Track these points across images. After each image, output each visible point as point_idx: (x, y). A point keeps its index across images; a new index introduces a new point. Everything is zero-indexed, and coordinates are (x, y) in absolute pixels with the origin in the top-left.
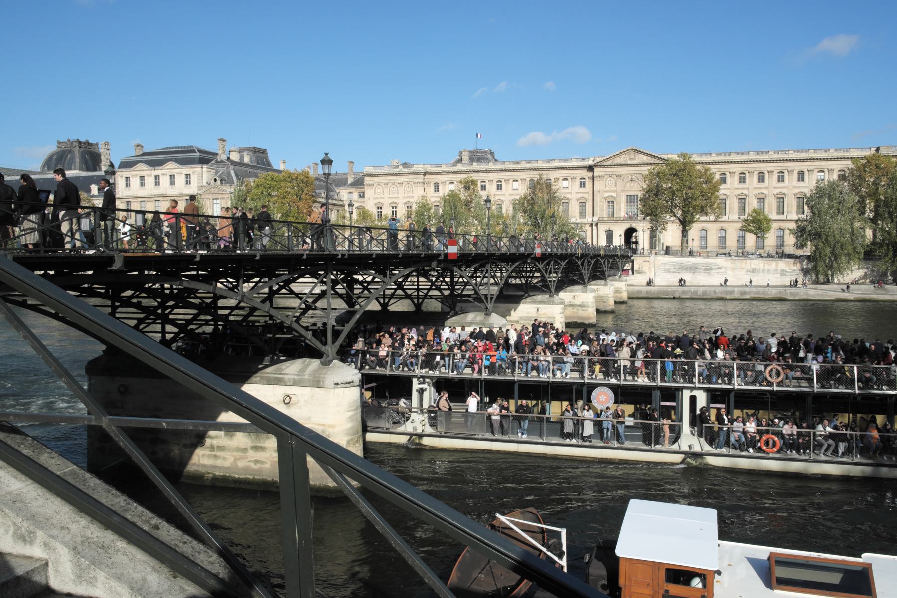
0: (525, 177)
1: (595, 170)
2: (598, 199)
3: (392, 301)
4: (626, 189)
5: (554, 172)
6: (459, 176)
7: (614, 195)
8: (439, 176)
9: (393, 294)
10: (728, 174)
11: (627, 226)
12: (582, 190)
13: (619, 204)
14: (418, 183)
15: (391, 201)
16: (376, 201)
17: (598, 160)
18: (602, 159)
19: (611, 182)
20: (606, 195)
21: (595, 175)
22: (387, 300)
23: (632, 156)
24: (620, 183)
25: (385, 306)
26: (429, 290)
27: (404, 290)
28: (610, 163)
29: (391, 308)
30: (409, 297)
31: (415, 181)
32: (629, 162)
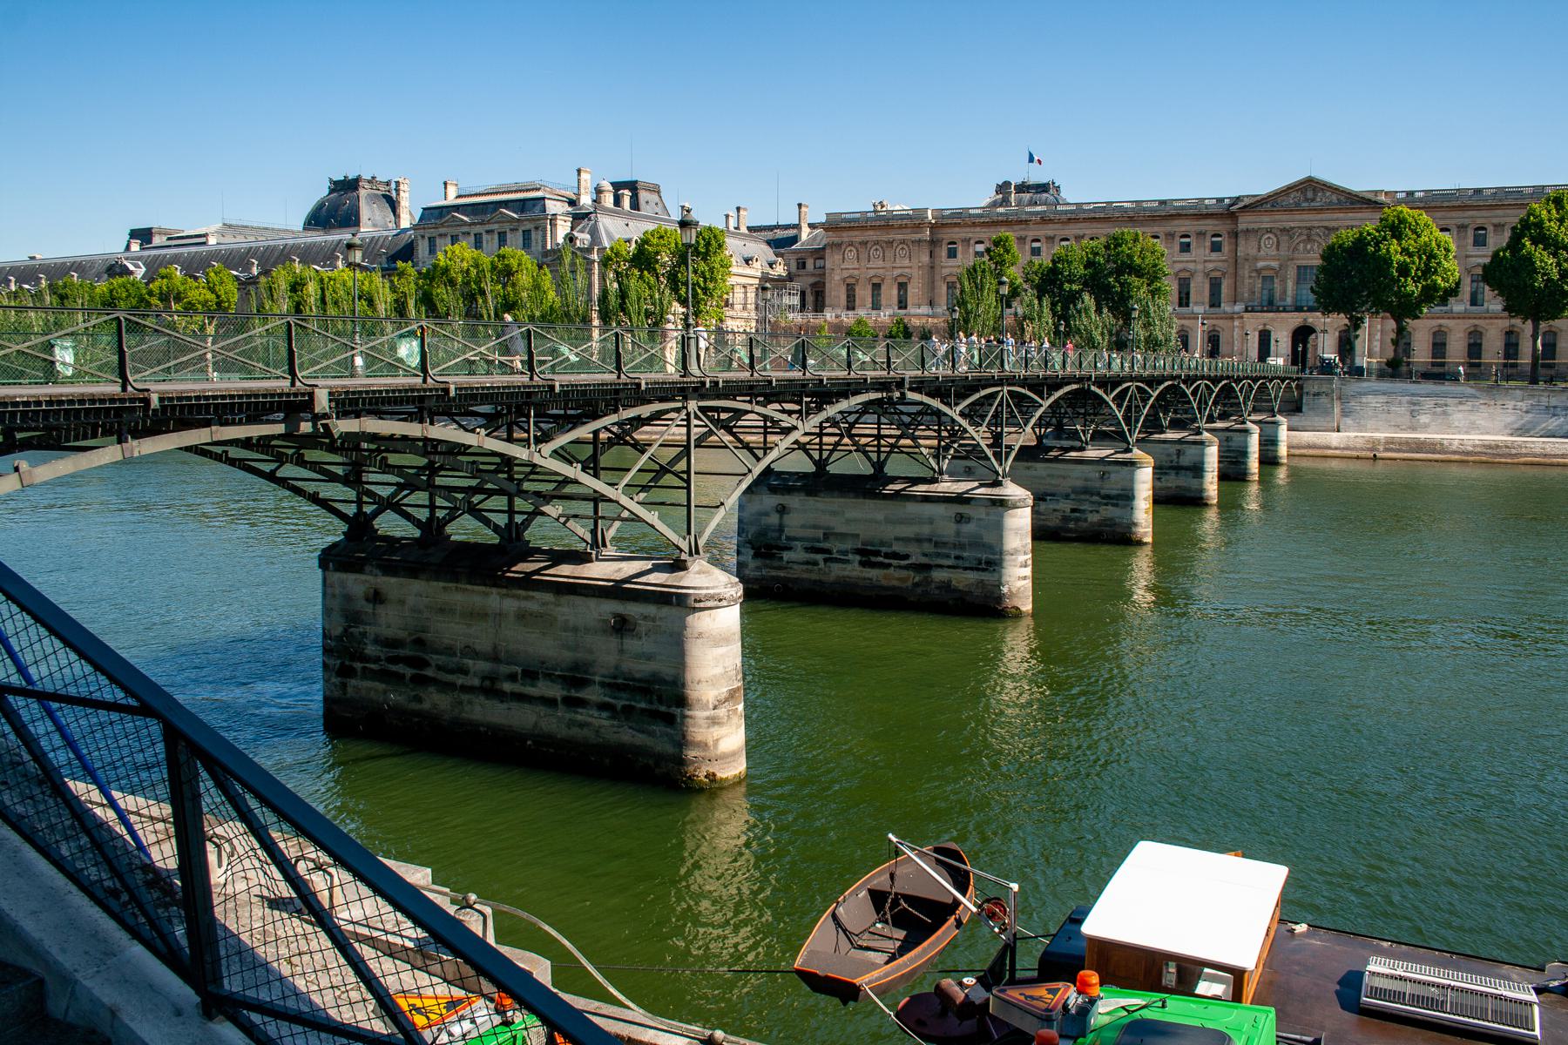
2: (1245, 272)
3: (836, 455)
7: (1275, 264)
9: (837, 444)
10: (1490, 228)
11: (1296, 320)
12: (1214, 256)
13: (1284, 281)
15: (872, 273)
16: (846, 274)
17: (1247, 201)
19: (1268, 242)
20: (1260, 264)
21: (1241, 226)
22: (825, 454)
23: (1310, 195)
25: (821, 464)
26: (899, 437)
27: (851, 437)
29: (832, 469)
30: (861, 449)
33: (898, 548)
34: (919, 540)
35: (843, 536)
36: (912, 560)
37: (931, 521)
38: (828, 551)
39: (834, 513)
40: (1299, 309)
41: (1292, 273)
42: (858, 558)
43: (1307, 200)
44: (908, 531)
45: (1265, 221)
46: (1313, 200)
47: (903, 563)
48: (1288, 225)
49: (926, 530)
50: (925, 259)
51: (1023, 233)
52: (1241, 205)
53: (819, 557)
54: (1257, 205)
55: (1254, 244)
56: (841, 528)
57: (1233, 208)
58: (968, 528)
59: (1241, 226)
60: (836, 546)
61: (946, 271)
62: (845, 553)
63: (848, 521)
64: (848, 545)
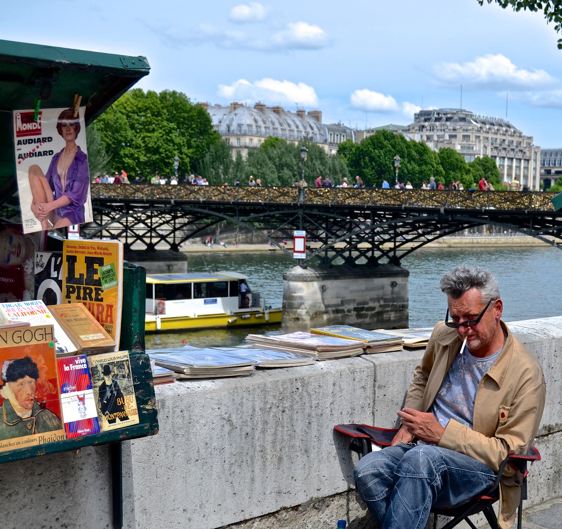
33: (371, 304)
34: (378, 299)
35: (349, 302)
36: (376, 310)
37: (383, 287)
38: (343, 311)
39: (346, 288)
42: (355, 313)
44: (374, 294)
47: (373, 312)
49: (381, 293)
53: (340, 315)
56: (349, 297)
58: (396, 289)
60: (346, 308)
62: (349, 311)
63: (352, 292)
64: (352, 306)
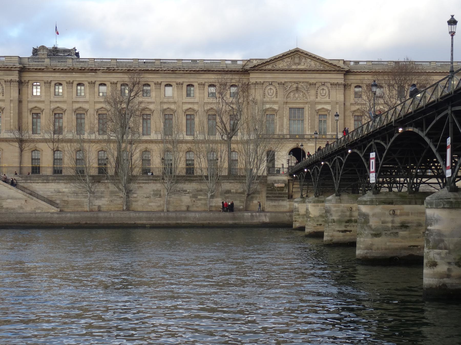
0: (160, 81)
1: (252, 75)
4: (289, 100)
5: (198, 76)
6: (69, 75)
7: (276, 107)
8: (40, 74)
13: (281, 118)
14: (11, 81)
17: (255, 63)
18: (260, 62)
19: (271, 91)
23: (297, 60)
24: (281, 93)
28: (269, 67)
31: (9, 78)
32: (294, 67)
40: (293, 137)
41: (286, 113)
43: (295, 64)
45: (268, 77)
46: (299, 64)
48: (283, 81)
50: (15, 94)
51: (93, 80)
52: (251, 65)
54: (261, 67)
55: (261, 92)
57: (248, 67)
59: (252, 81)
61: (31, 106)
